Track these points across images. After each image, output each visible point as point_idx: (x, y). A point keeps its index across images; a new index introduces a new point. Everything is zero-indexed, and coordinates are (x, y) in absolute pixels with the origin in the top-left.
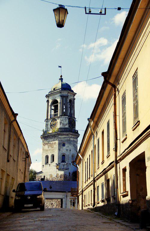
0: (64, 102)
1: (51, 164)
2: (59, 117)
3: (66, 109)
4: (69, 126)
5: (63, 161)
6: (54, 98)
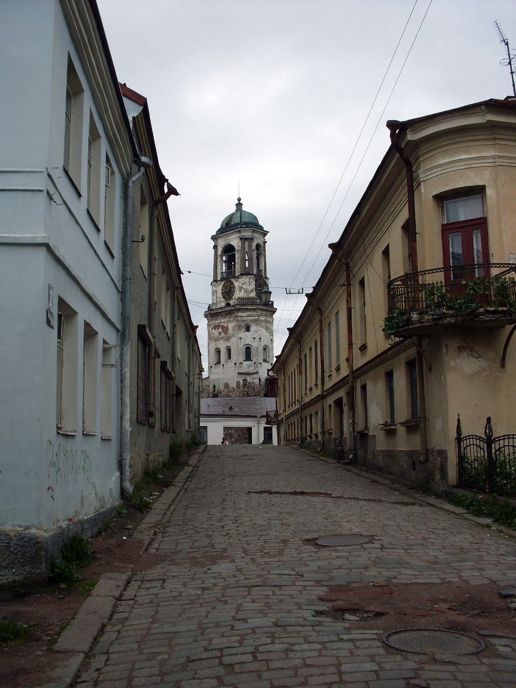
0: (247, 250)
1: (224, 364)
2: (238, 277)
3: (250, 260)
4: (257, 294)
5: (248, 357)
6: (227, 242)
